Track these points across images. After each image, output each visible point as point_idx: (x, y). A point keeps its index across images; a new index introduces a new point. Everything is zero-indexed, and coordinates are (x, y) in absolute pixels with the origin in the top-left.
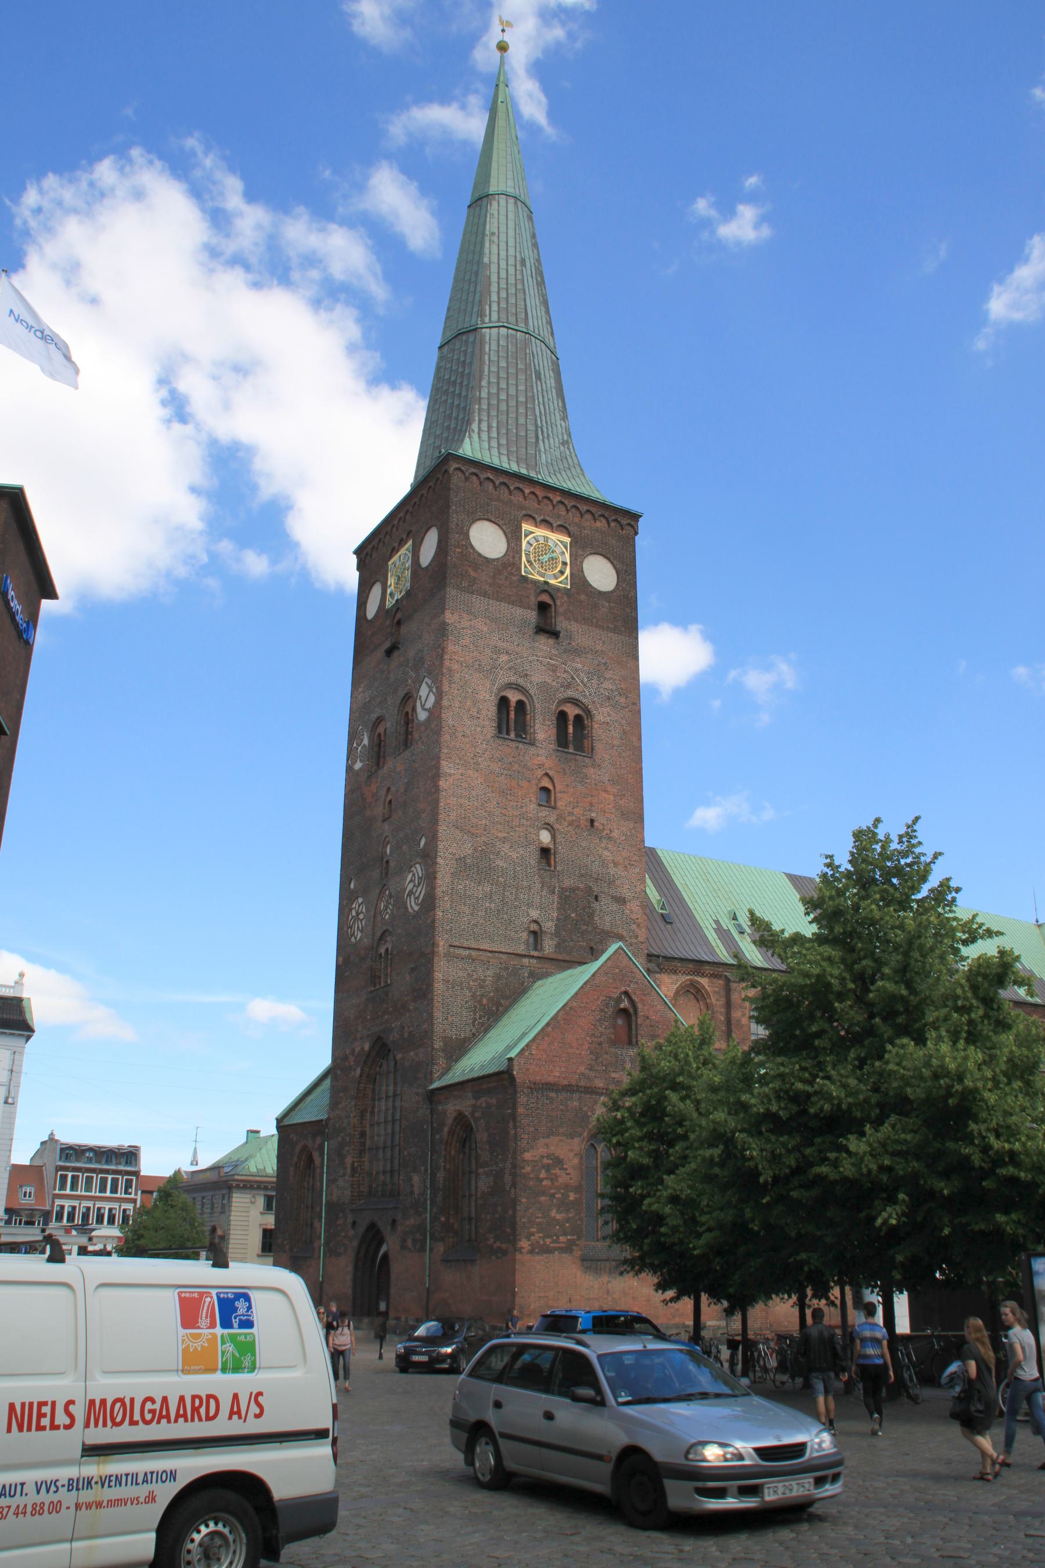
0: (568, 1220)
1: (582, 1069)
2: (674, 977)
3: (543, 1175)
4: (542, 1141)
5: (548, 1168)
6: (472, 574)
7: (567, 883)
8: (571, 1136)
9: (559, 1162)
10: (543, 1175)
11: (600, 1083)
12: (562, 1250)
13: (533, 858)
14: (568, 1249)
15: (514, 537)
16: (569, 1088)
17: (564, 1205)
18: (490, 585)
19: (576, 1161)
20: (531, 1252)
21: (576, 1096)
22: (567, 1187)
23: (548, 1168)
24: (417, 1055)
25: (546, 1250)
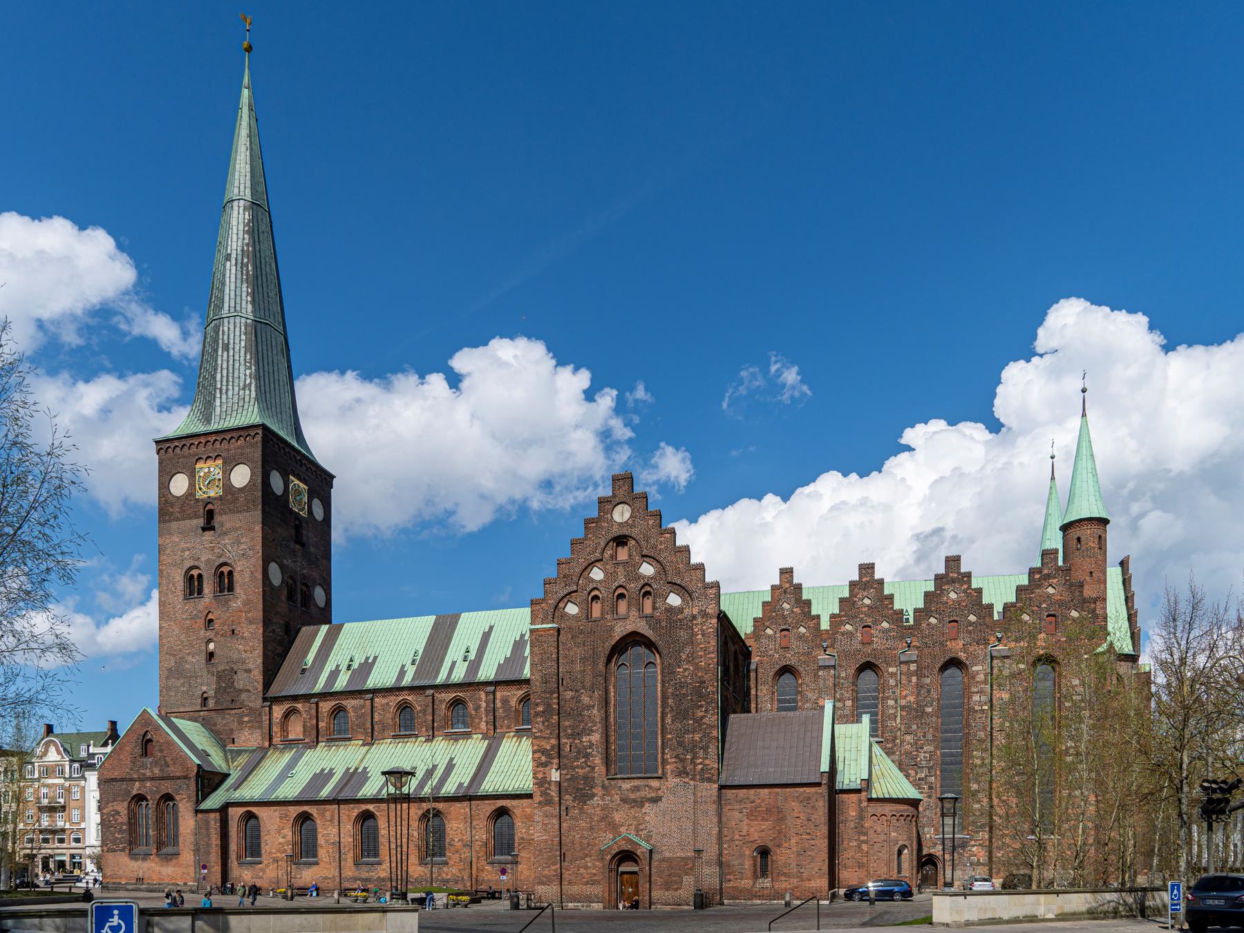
0: (123, 838)
1: (127, 770)
2: (282, 707)
3: (111, 819)
4: (111, 804)
5: (113, 816)
6: (171, 510)
7: (221, 668)
8: (123, 801)
9: (118, 813)
10: (111, 819)
11: (135, 776)
12: (121, 850)
13: (202, 658)
14: (123, 850)
15: (192, 475)
16: (123, 780)
17: (121, 831)
18: (180, 513)
19: (126, 812)
20: (108, 851)
21: (125, 783)
22: (122, 823)
23: (113, 816)
24: (49, 771)
25: (114, 851)
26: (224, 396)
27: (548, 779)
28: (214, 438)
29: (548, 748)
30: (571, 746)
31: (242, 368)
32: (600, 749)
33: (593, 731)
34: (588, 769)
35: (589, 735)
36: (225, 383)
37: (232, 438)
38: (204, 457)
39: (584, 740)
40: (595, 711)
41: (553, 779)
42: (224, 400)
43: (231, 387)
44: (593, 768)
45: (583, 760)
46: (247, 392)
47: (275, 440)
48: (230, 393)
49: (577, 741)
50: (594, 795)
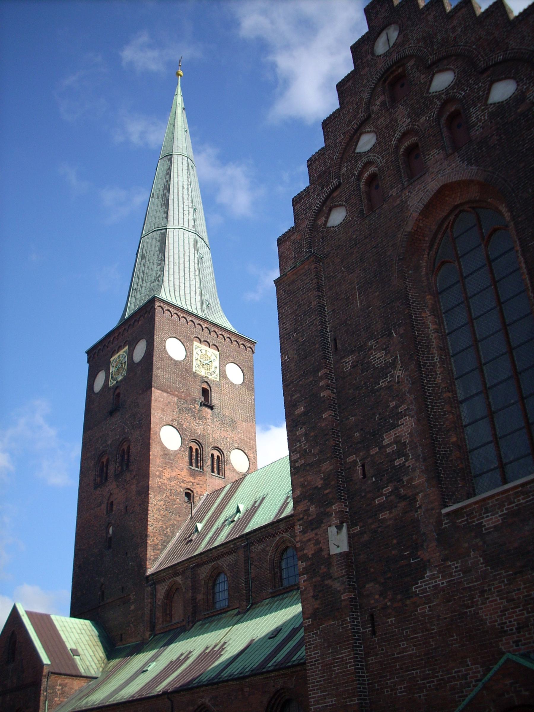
26: (138, 293)
27: (324, 553)
28: (123, 328)
29: (319, 483)
30: (363, 466)
31: (155, 266)
32: (419, 450)
33: (401, 416)
34: (402, 505)
35: (394, 426)
36: (140, 283)
37: (135, 321)
38: (117, 349)
39: (386, 442)
40: (398, 373)
41: (334, 550)
42: (138, 297)
43: (144, 285)
44: (413, 499)
45: (390, 489)
46: (157, 283)
47: (173, 311)
48: (144, 288)
49: (374, 451)
50: (423, 566)
